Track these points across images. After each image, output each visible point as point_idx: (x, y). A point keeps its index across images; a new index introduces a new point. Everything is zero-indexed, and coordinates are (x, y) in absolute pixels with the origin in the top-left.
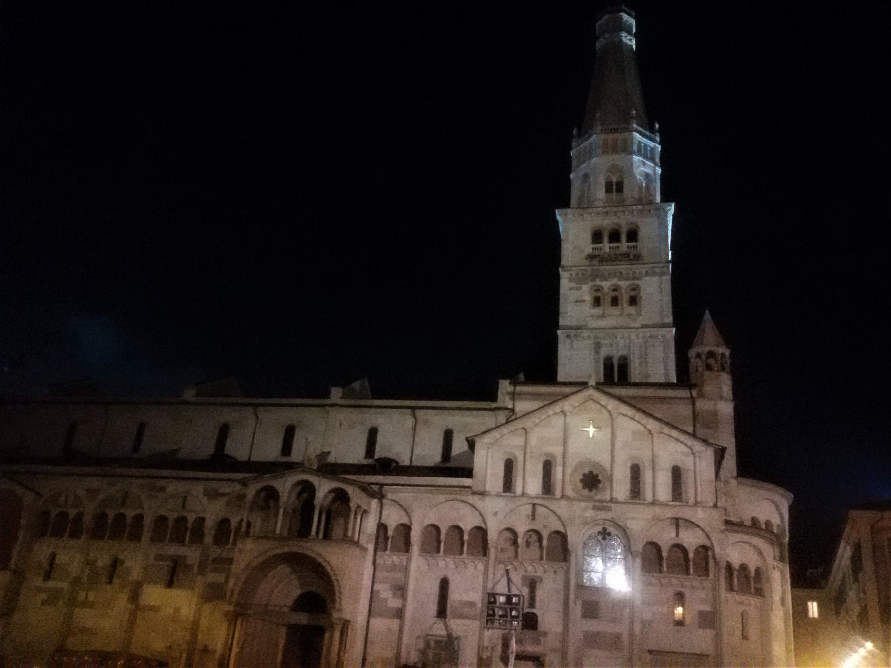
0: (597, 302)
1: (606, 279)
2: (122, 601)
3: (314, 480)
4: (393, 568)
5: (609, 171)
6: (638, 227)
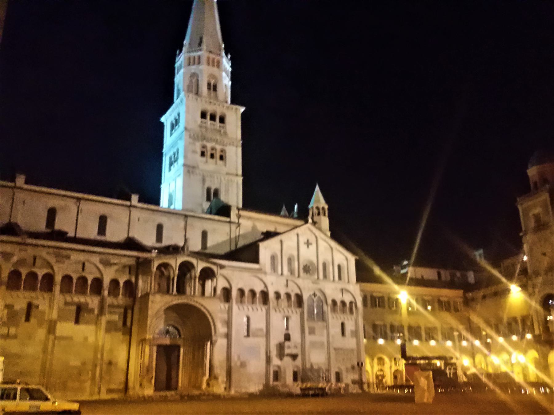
0: (203, 154)
2: (41, 333)
3: (194, 261)
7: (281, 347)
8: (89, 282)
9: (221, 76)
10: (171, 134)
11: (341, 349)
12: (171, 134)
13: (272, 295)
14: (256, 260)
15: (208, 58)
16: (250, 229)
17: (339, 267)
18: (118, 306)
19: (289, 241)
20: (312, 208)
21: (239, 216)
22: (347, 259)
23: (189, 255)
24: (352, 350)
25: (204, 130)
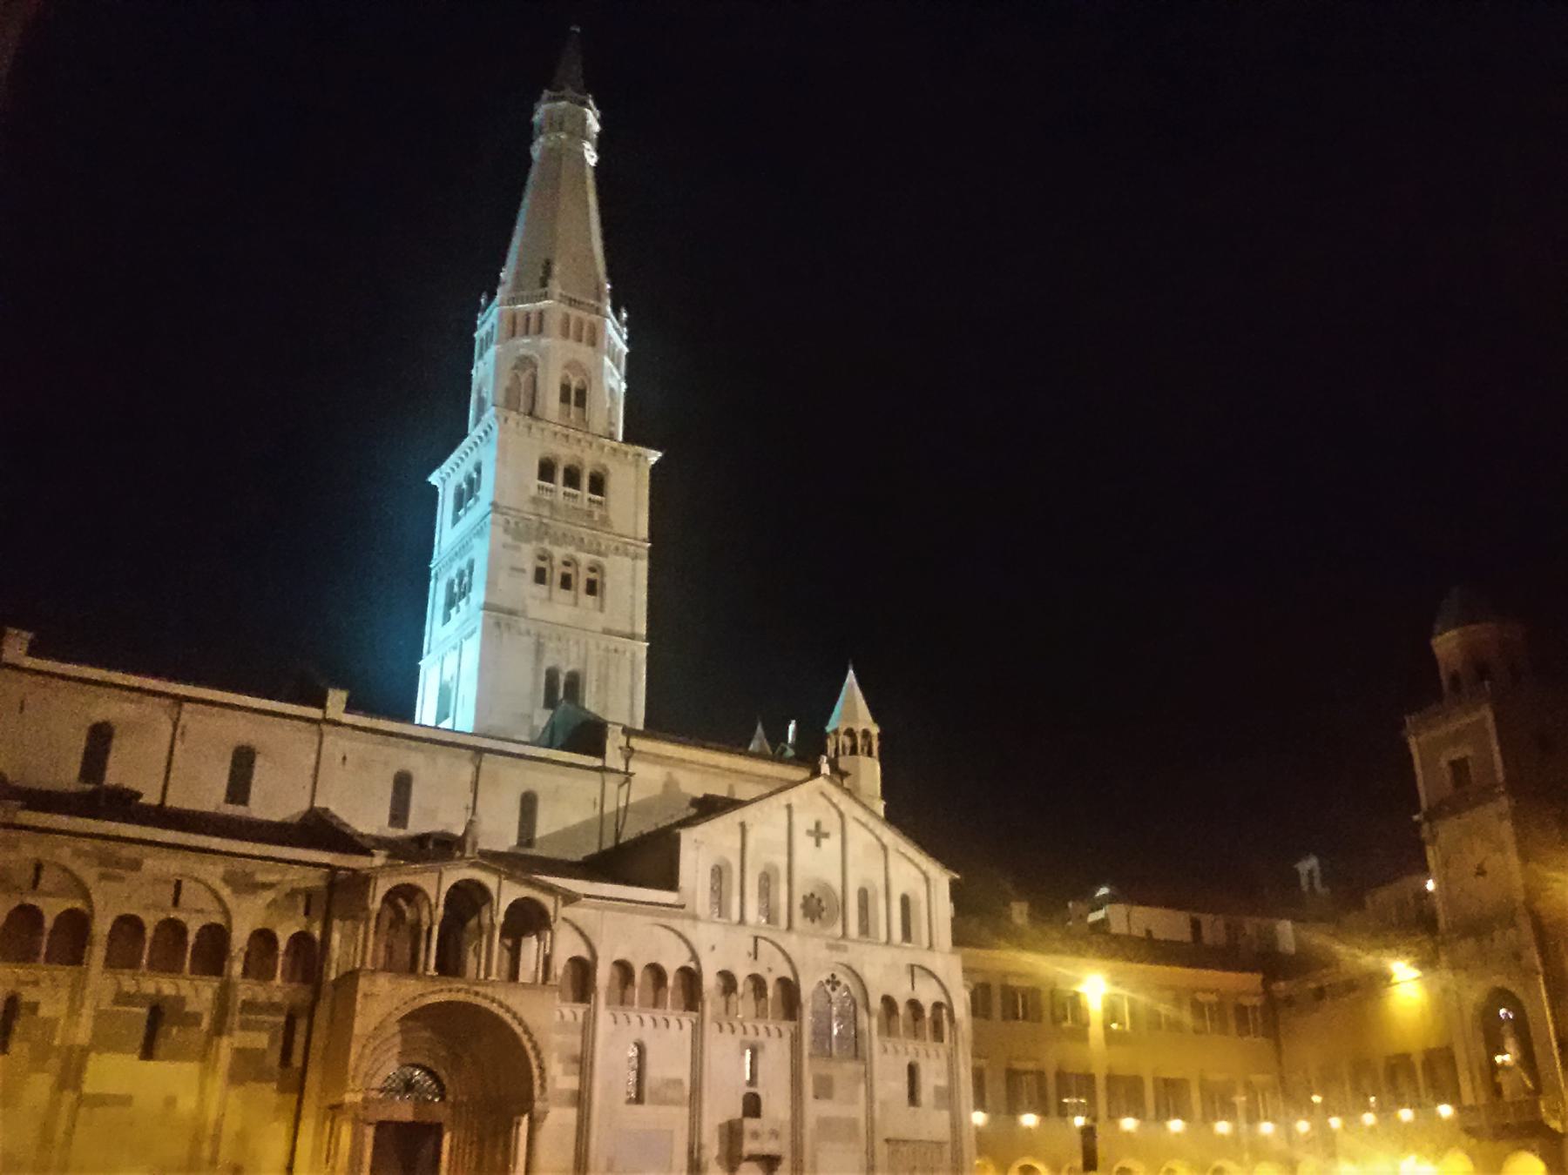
0: (540, 577)
1: (560, 545)
2: (40, 1087)
3: (490, 881)
4: (563, 1026)
5: (567, 367)
6: (606, 470)
7: (732, 1134)
8: (191, 938)
9: (601, 365)
10: (456, 519)
11: (905, 1142)
12: (456, 519)
13: (710, 981)
14: (669, 880)
15: (567, 319)
16: (658, 790)
17: (905, 901)
18: (272, 1007)
19: (766, 825)
20: (836, 732)
21: (629, 753)
22: (927, 880)
23: (474, 865)
24: (940, 1144)
25: (546, 511)
